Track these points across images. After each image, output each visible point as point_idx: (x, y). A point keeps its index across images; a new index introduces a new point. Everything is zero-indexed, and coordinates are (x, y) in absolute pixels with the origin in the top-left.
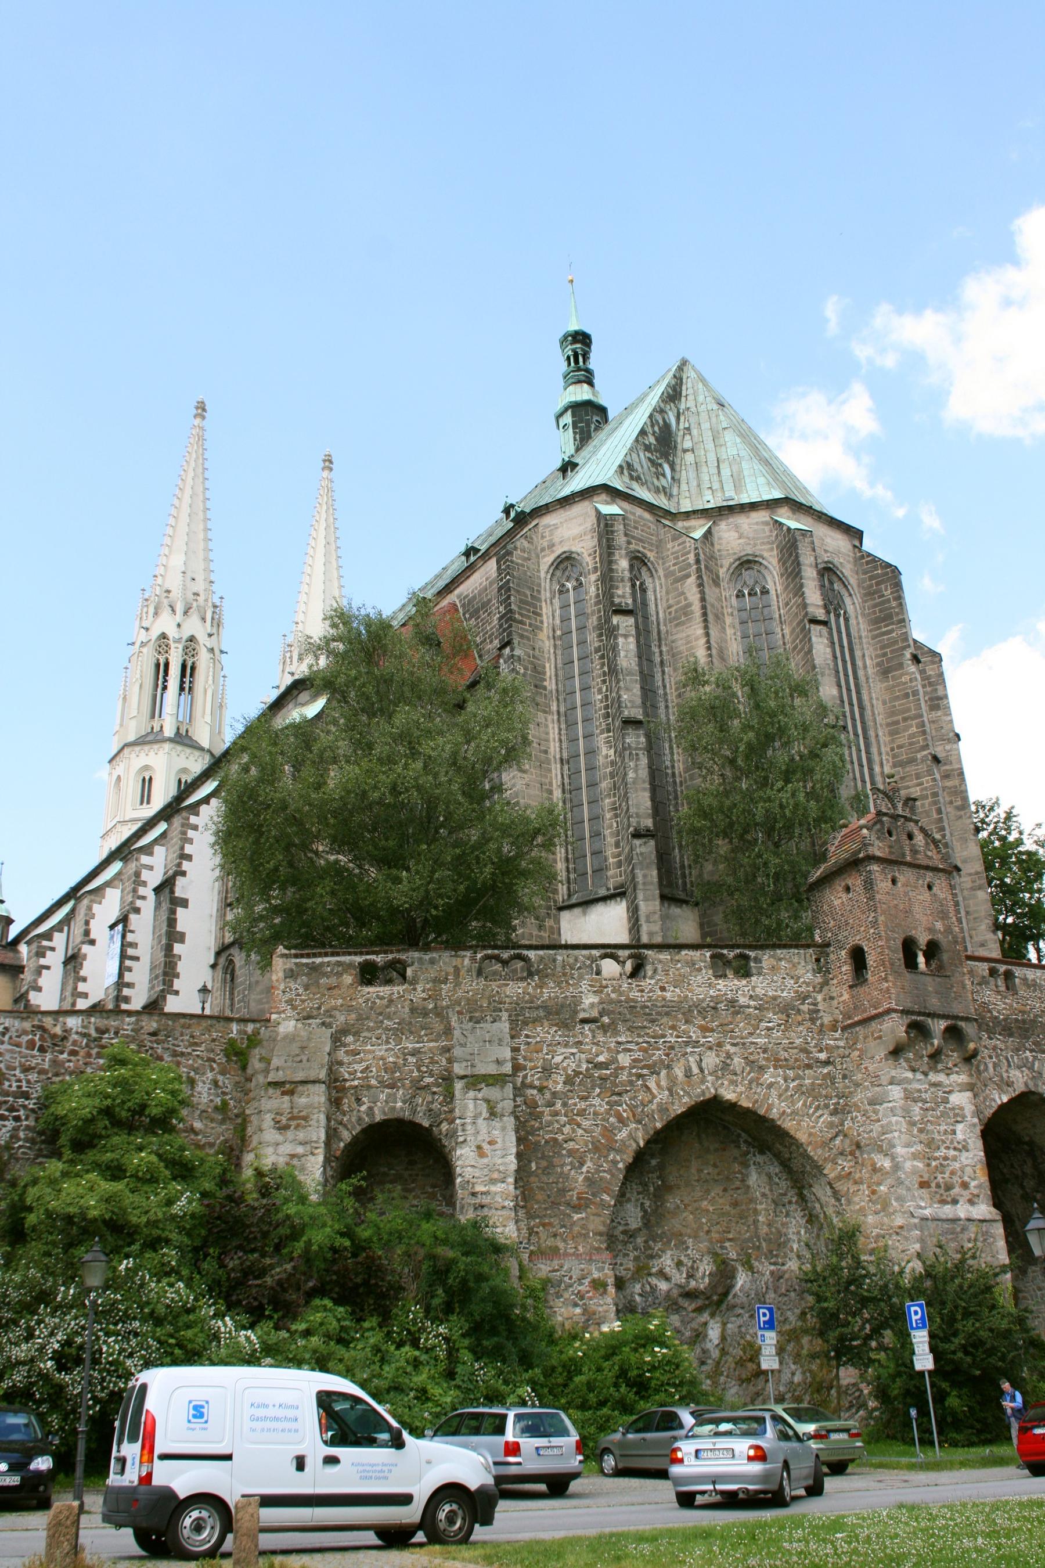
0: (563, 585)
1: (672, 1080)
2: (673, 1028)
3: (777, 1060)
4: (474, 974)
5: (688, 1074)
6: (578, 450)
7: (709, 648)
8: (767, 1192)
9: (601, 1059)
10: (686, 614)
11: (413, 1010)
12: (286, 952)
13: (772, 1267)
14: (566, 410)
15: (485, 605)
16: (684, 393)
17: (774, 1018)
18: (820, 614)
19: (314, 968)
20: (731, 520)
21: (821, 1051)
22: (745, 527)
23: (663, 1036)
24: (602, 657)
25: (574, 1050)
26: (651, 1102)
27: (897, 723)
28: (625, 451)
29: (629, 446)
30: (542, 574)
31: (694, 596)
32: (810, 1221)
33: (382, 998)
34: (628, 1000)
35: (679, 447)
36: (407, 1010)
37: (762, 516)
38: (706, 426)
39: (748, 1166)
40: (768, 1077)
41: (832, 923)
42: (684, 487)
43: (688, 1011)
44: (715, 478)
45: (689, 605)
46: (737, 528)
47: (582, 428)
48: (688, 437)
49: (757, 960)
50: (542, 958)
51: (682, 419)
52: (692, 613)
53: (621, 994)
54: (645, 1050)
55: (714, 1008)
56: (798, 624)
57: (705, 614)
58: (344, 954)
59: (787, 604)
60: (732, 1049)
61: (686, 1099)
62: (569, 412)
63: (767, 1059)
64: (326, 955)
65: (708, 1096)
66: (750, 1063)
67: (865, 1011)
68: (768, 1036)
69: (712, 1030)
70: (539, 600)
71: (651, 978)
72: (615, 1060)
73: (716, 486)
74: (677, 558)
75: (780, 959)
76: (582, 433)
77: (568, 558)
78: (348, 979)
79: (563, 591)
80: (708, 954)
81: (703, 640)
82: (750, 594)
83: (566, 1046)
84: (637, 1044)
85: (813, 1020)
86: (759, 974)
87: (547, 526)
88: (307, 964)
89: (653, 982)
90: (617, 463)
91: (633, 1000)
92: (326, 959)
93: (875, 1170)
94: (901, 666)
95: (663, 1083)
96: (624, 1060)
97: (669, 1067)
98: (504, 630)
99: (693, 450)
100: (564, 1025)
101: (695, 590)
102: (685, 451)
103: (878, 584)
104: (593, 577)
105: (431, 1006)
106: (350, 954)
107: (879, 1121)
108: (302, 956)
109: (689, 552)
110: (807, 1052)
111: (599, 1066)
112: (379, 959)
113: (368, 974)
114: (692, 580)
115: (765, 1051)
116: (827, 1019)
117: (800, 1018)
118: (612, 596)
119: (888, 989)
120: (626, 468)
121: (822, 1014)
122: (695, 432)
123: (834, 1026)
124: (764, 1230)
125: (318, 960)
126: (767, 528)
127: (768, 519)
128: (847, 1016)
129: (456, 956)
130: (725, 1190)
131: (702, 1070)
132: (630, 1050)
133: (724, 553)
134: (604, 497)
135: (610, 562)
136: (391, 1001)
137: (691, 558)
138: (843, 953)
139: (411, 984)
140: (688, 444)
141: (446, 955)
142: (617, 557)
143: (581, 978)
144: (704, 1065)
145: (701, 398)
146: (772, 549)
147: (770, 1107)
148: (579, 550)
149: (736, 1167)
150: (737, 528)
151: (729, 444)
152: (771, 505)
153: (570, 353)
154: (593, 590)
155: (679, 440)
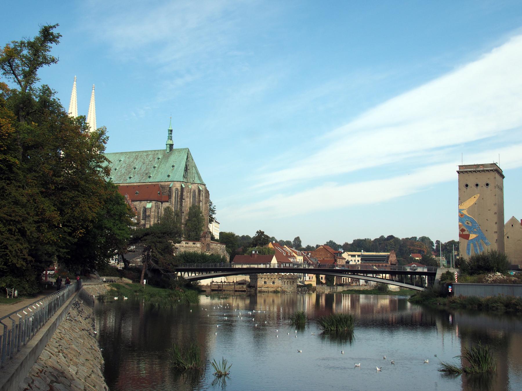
28: (183, 173)
31: (189, 196)
37: (197, 185)
38: (191, 165)
90: (183, 175)
140: (189, 168)
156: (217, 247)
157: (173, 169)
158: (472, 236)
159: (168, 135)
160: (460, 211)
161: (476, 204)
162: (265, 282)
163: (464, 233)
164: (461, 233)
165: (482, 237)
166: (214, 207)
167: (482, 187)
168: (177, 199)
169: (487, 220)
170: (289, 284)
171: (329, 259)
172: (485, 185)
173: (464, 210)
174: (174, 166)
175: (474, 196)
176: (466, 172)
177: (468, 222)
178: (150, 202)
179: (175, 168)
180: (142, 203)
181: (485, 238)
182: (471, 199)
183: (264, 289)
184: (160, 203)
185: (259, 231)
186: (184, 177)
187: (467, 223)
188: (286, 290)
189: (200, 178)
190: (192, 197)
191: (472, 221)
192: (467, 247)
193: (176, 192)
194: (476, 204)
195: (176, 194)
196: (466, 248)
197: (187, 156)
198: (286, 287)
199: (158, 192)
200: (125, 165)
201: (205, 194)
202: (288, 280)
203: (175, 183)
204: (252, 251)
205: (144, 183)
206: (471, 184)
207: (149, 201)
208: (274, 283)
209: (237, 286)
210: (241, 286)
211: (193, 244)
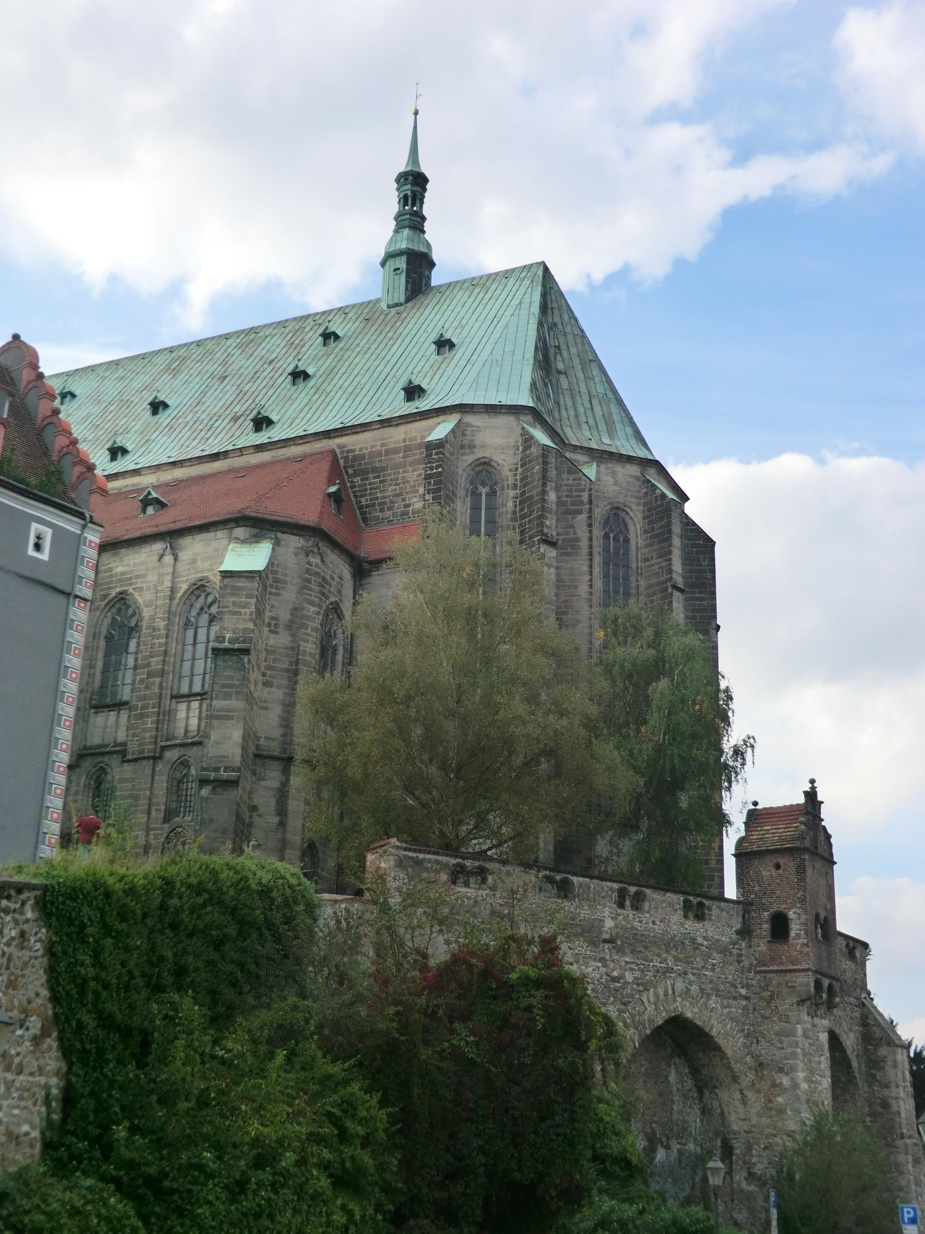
0: (476, 488)
1: (656, 995)
2: (659, 956)
3: (718, 990)
4: (537, 890)
5: (666, 995)
6: (408, 300)
7: (591, 586)
8: (680, 1087)
9: (615, 974)
10: (573, 547)
11: (493, 913)
12: (398, 844)
13: (679, 1146)
14: (400, 253)
15: (378, 471)
16: (550, 306)
17: (716, 958)
18: (679, 580)
19: (418, 863)
20: (610, 465)
21: (743, 987)
22: (620, 476)
23: (652, 961)
25: (600, 965)
26: (644, 1013)
29: (531, 362)
30: (460, 471)
31: (583, 534)
32: (703, 1113)
33: (469, 898)
34: (633, 928)
35: (553, 365)
36: (488, 912)
37: (634, 470)
38: (574, 350)
39: (669, 1065)
40: (712, 1004)
41: (757, 888)
42: (564, 413)
43: (669, 944)
44: (589, 413)
45: (578, 540)
46: (614, 474)
48: (559, 357)
49: (709, 909)
50: (581, 885)
51: (551, 333)
52: (579, 548)
53: (628, 922)
54: (642, 971)
55: (683, 943)
56: (659, 583)
57: (591, 554)
58: (442, 855)
59: (646, 560)
60: (692, 978)
61: (664, 1014)
62: (404, 258)
63: (712, 989)
64: (429, 853)
65: (678, 1013)
66: (702, 990)
67: (782, 963)
68: (713, 970)
69: (681, 961)
70: (454, 494)
71: (648, 912)
72: (622, 977)
73: (592, 423)
74: (571, 491)
75: (722, 910)
76: (414, 284)
77: (485, 463)
78: (444, 877)
79: (475, 495)
80: (682, 899)
81: (587, 578)
82: (614, 538)
83: (595, 960)
84: (638, 965)
85: (739, 962)
86: (710, 920)
87: (469, 425)
88: (412, 858)
89: (648, 915)
91: (636, 929)
92: (428, 856)
93: (774, 1085)
95: (651, 999)
96: (629, 977)
97: (655, 987)
99: (565, 373)
100: (593, 943)
101: (585, 527)
102: (559, 372)
103: (697, 552)
104: (512, 493)
105: (506, 912)
106: (447, 855)
107: (783, 1048)
108: (410, 850)
109: (583, 490)
110: (736, 987)
111: (615, 980)
112: (468, 863)
113: (458, 875)
114: (583, 517)
115: (711, 982)
116: (746, 963)
117: (732, 959)
118: (542, 525)
119: (807, 954)
120: (533, 385)
121: (743, 958)
122: (565, 353)
123: (750, 969)
124: (675, 1116)
125: (421, 856)
126: (637, 483)
127: (639, 474)
128: (761, 962)
129: (524, 872)
130: (656, 1083)
131: (674, 992)
132: (633, 970)
133: (601, 494)
134: (529, 418)
135: (544, 492)
136: (476, 902)
137: (585, 497)
138: (766, 914)
139: (491, 889)
140: (560, 366)
141: (518, 869)
142: (548, 489)
143: (604, 906)
144: (676, 988)
146: (639, 505)
147: (711, 1028)
148: (501, 462)
149: (663, 1066)
150: (614, 474)
151: (597, 379)
153: (409, 193)
154: (510, 504)
155: (552, 356)
159: (395, 208)
174: (452, 345)
178: (255, 539)
180: (184, 555)
184: (346, 571)
190: (597, 559)
193: (475, 495)
195: (476, 508)
199: (333, 489)
200: (96, 410)
203: (470, 419)
205: (216, 456)
207: (240, 532)
211: (687, 906)
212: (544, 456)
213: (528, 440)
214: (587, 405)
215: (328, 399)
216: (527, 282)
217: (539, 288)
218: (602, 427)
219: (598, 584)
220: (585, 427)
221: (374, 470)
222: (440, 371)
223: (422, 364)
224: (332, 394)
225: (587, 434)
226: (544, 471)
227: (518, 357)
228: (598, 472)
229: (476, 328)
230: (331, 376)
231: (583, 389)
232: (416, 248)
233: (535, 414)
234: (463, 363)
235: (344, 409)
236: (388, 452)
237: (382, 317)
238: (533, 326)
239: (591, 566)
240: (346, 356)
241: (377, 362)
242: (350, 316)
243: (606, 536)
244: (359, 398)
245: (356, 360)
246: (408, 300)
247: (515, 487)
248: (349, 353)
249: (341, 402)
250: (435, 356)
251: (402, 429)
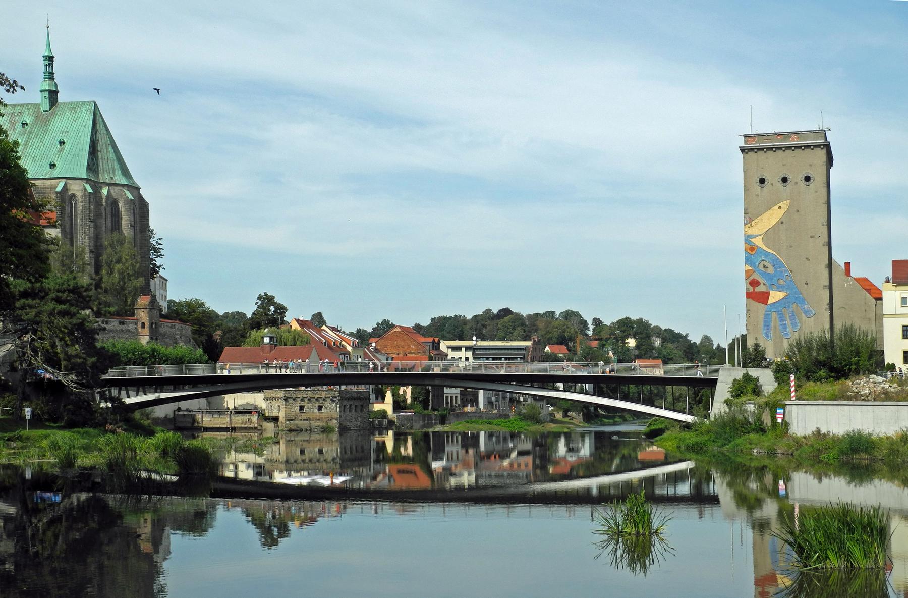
14: (46, 91)
22: (116, 190)
24: (82, 228)
27: (142, 246)
38: (104, 141)
44: (107, 166)
45: (102, 214)
47: (52, 101)
56: (127, 224)
62: (48, 92)
73: (108, 171)
76: (52, 103)
87: (68, 183)
94: (146, 231)
98: (58, 215)
104: (81, 204)
135: (90, 207)
145: (101, 126)
150: (114, 189)
152: (123, 185)
156: (173, 330)
157: (61, 150)
158: (776, 296)
160: (748, 239)
161: (782, 223)
162: (302, 408)
163: (758, 289)
164: (751, 289)
165: (794, 299)
166: (160, 242)
167: (796, 183)
168: (76, 220)
169: (807, 259)
170: (353, 411)
171: (413, 355)
172: (803, 181)
173: (756, 236)
174: (64, 143)
175: (780, 205)
176: (761, 149)
177: (767, 264)
179: (67, 146)
181: (804, 300)
182: (770, 212)
183: (302, 422)
185: (263, 294)
186: (89, 168)
187: (765, 266)
188: (348, 424)
189: (126, 172)
190: (109, 216)
191: (776, 263)
192: (765, 322)
194: (782, 223)
196: (762, 324)
197: (94, 120)
198: (348, 419)
201: (140, 208)
202: (351, 402)
203: (68, 181)
204: (263, 337)
206: (773, 178)
208: (320, 408)
209: (237, 418)
210: (245, 418)
212: (89, 196)
213: (85, 189)
214: (107, 163)
215: (26, 160)
216: (88, 112)
217: (92, 117)
218: (111, 171)
219: (109, 224)
220: (106, 172)
221: (42, 193)
222: (60, 156)
223: (55, 149)
224: (27, 157)
225: (106, 175)
226: (89, 200)
227: (84, 153)
228: (109, 189)
229: (72, 134)
230: (26, 146)
231: (106, 158)
232: (51, 89)
233: (87, 180)
234: (67, 153)
235: (32, 166)
236: (46, 188)
237: (42, 116)
238: (89, 134)
239: (106, 222)
240: (30, 137)
241: (41, 144)
242: (31, 111)
243: (112, 209)
244: (36, 162)
245: (34, 140)
246: (50, 110)
247: (82, 202)
248: (31, 135)
249: (31, 162)
250: (59, 147)
251: (49, 181)
